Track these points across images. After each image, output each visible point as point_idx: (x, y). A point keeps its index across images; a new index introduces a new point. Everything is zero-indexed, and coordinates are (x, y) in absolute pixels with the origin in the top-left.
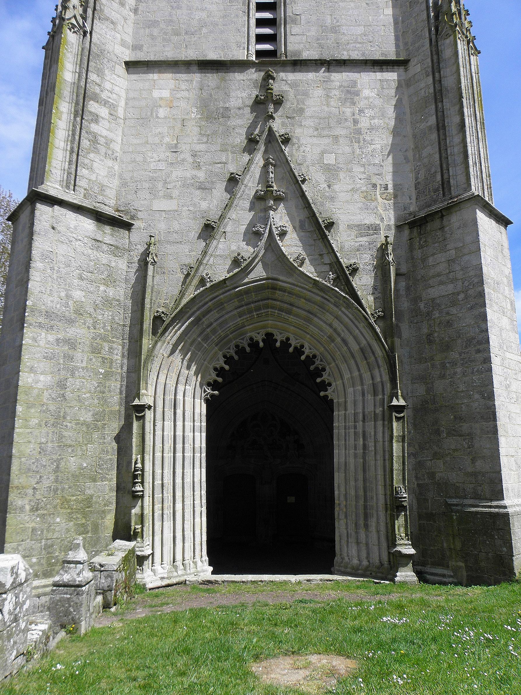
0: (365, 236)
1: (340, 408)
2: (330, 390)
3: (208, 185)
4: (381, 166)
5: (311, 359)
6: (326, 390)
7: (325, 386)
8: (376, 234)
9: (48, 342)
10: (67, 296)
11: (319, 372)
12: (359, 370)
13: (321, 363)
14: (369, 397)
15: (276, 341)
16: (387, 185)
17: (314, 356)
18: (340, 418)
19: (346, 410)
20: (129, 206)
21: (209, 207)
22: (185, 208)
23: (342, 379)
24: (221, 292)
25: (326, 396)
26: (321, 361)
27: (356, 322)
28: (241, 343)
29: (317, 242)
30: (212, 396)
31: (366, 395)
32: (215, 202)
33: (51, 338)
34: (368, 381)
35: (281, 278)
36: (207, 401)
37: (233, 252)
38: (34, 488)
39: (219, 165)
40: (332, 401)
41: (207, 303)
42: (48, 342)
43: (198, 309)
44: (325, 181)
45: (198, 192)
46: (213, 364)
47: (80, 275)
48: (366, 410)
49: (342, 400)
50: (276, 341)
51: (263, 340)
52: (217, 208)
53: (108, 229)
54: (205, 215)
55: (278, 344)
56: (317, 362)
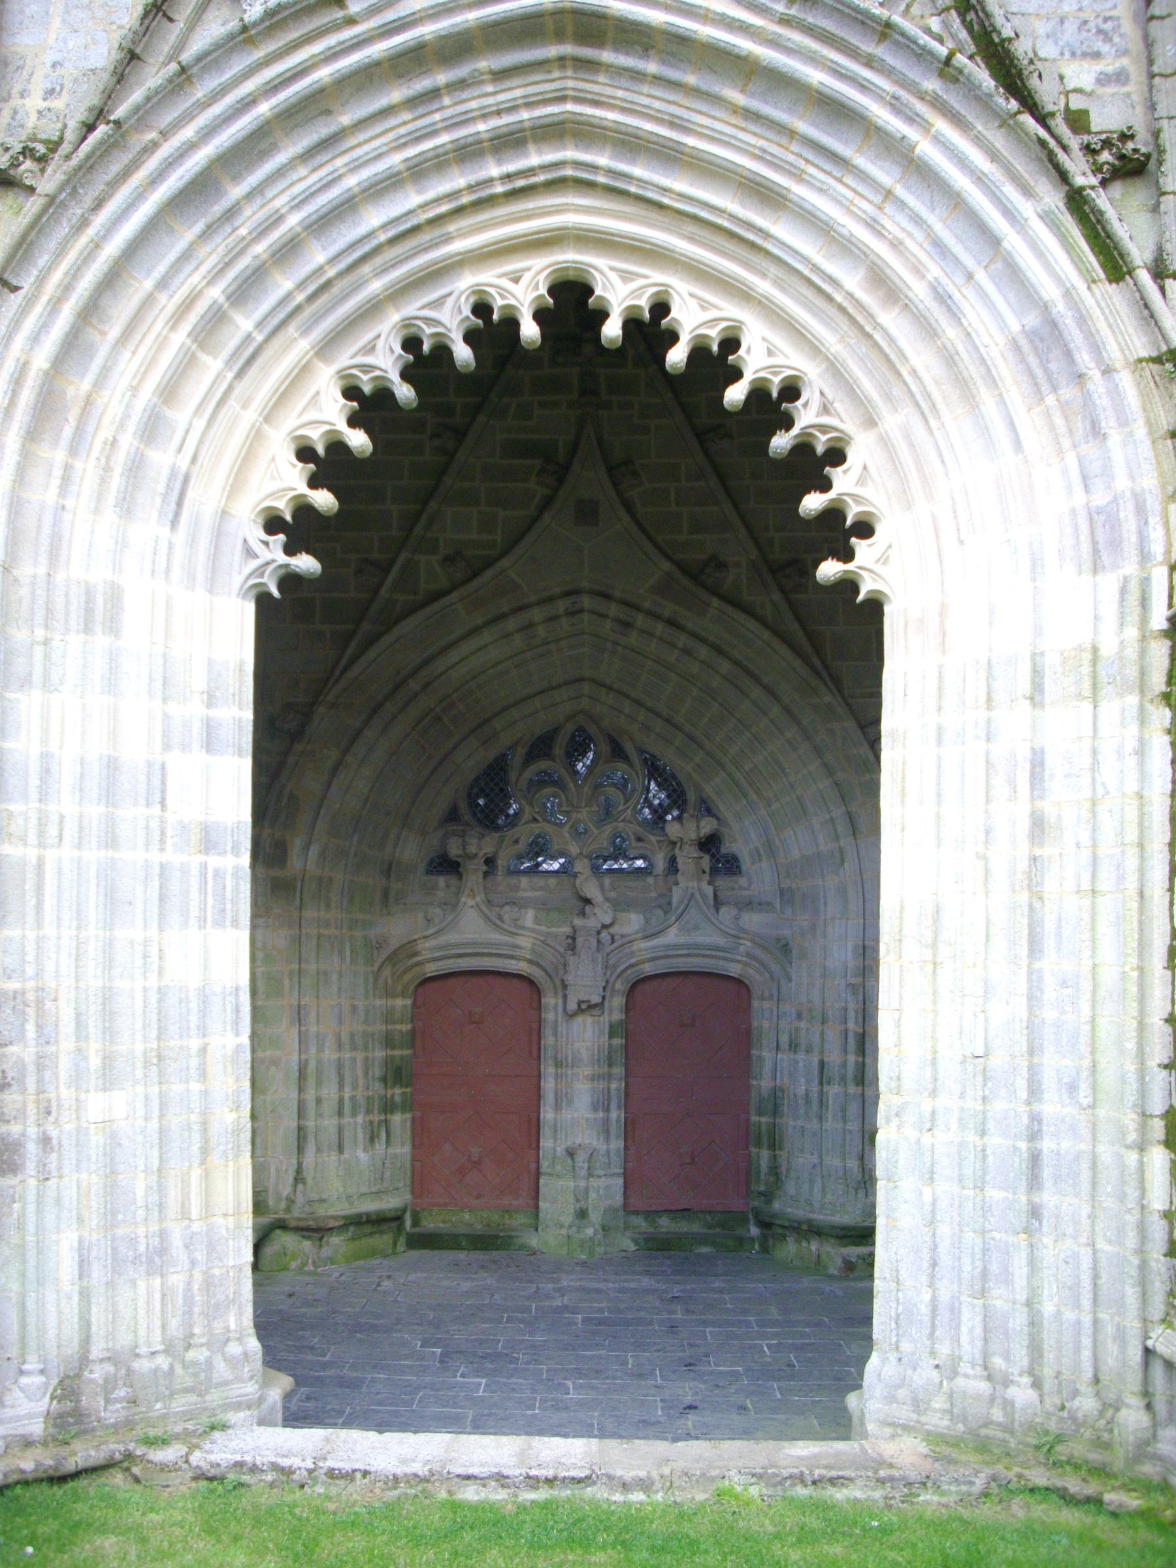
6: (847, 555)
13: (825, 420)
15: (602, 315)
24: (317, 48)
25: (849, 585)
26: (825, 409)
27: (1010, 191)
28: (428, 321)
36: (263, 601)
40: (875, 607)
43: (208, 133)
51: (540, 316)
55: (612, 330)
56: (806, 415)
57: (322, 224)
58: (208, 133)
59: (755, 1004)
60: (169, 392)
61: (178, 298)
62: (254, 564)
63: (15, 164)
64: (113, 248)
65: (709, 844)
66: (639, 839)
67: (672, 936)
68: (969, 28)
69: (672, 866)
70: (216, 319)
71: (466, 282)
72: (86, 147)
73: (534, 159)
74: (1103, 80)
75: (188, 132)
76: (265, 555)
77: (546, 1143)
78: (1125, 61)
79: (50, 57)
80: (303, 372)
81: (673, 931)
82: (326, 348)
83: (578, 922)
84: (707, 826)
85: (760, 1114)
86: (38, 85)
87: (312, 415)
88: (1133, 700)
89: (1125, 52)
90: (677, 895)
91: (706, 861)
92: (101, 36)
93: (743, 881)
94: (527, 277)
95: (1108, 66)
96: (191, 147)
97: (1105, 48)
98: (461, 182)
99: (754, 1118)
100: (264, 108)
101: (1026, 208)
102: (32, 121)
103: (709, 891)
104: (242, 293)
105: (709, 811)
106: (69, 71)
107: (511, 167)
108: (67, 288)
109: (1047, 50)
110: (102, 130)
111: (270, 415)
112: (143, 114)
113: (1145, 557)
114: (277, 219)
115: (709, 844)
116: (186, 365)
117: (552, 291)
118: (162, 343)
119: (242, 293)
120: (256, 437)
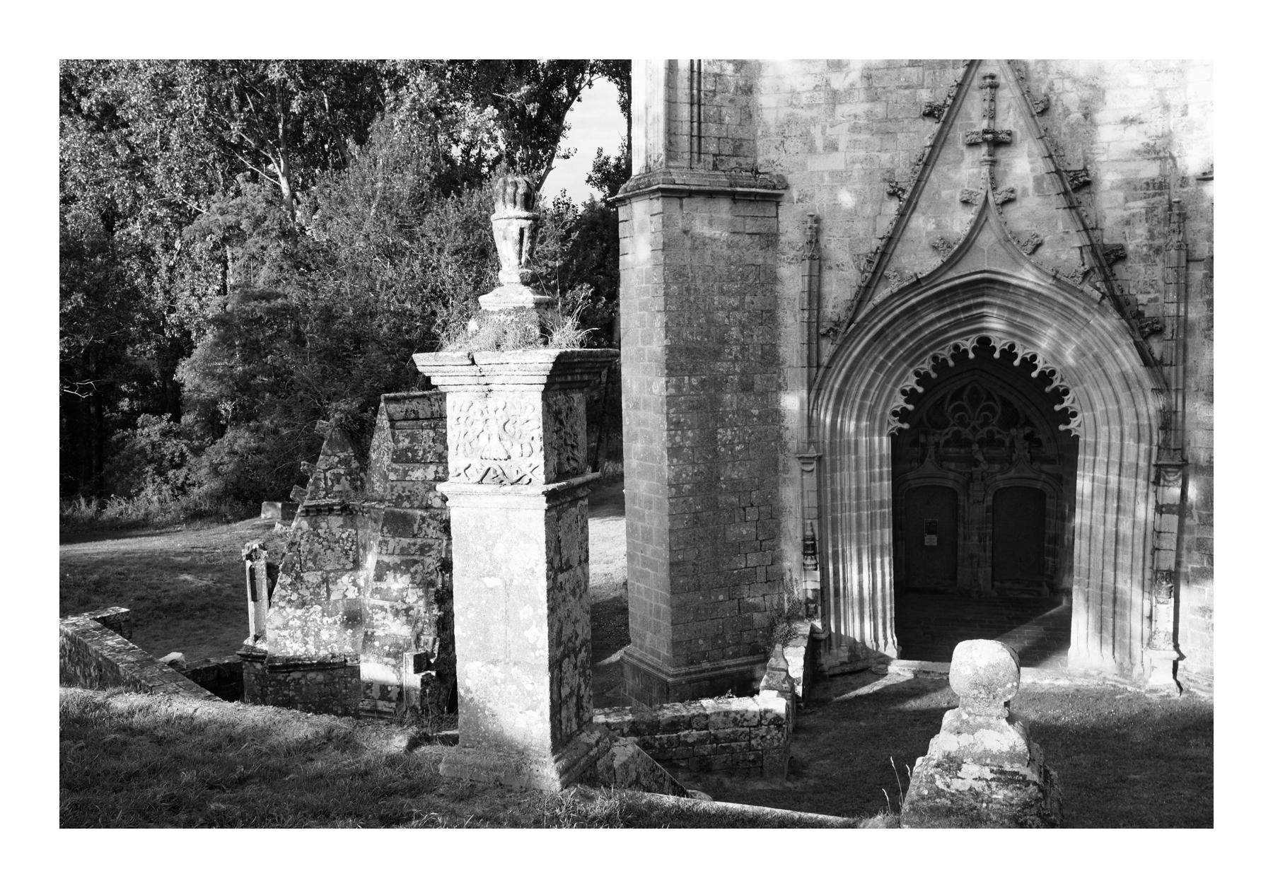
0: (1141, 199)
1: (1088, 451)
2: (1073, 424)
3: (891, 127)
4: (1180, 71)
5: (1047, 377)
7: (1067, 416)
8: (1160, 195)
9: (692, 387)
10: (707, 321)
11: (1060, 394)
12: (1118, 402)
13: (1062, 384)
14: (1130, 443)
16: (1186, 106)
17: (1053, 372)
18: (1087, 464)
19: (1095, 454)
20: (774, 165)
21: (892, 162)
22: (858, 166)
23: (1092, 409)
24: (912, 295)
29: (1061, 211)
30: (900, 430)
31: (1126, 438)
32: (903, 154)
33: (694, 381)
34: (1130, 420)
35: (1003, 271)
36: (892, 436)
37: (928, 234)
38: (694, 564)
39: (907, 92)
40: (1077, 437)
41: (893, 310)
42: (692, 387)
44: (1080, 107)
45: (876, 140)
46: (900, 386)
47: (721, 288)
48: (1125, 460)
49: (1090, 439)
50: (994, 349)
51: (974, 349)
52: (905, 164)
53: (750, 210)
54: (887, 176)
57: (911, 336)
58: (880, 320)
59: (1048, 500)
60: (869, 385)
61: (871, 359)
62: (891, 427)
63: (828, 332)
64: (855, 354)
65: (1028, 437)
66: (999, 433)
67: (1012, 473)
68: (1107, 287)
69: (1012, 442)
70: (883, 364)
71: (952, 343)
72: (849, 330)
73: (974, 312)
74: (1150, 301)
75: (876, 320)
76: (895, 425)
77: (960, 553)
78: (1157, 294)
79: (834, 295)
80: (905, 372)
81: (1013, 471)
82: (911, 365)
83: (973, 469)
84: (1028, 430)
85: (1048, 556)
86: (830, 305)
87: (907, 383)
88: (1145, 483)
89: (1158, 291)
90: (1014, 456)
91: (1027, 444)
92: (848, 289)
93: (1043, 450)
94: (971, 340)
95: (1152, 296)
96: (877, 324)
97: (1152, 290)
98: (952, 320)
99: (1046, 545)
100: (897, 311)
101: (1123, 342)
102: (830, 315)
103: (1028, 455)
104: (888, 357)
105: (1028, 422)
106: (841, 300)
107: (967, 315)
108: (843, 365)
109: (1133, 291)
110: (853, 326)
111: (895, 385)
112: (864, 320)
113: (1151, 442)
114: (898, 335)
115: (1028, 437)
116: (874, 377)
117: (978, 342)
118: (867, 372)
119: (888, 357)
120: (892, 391)
